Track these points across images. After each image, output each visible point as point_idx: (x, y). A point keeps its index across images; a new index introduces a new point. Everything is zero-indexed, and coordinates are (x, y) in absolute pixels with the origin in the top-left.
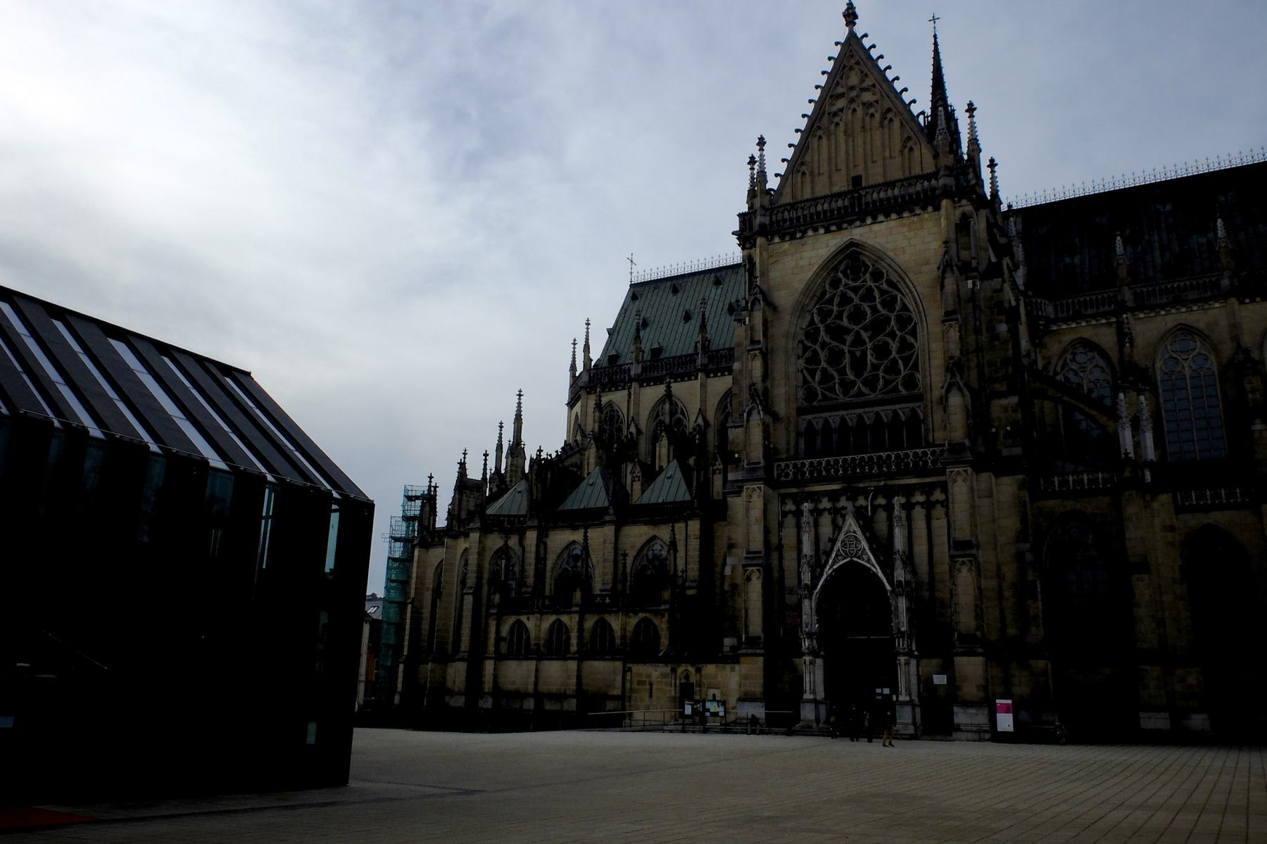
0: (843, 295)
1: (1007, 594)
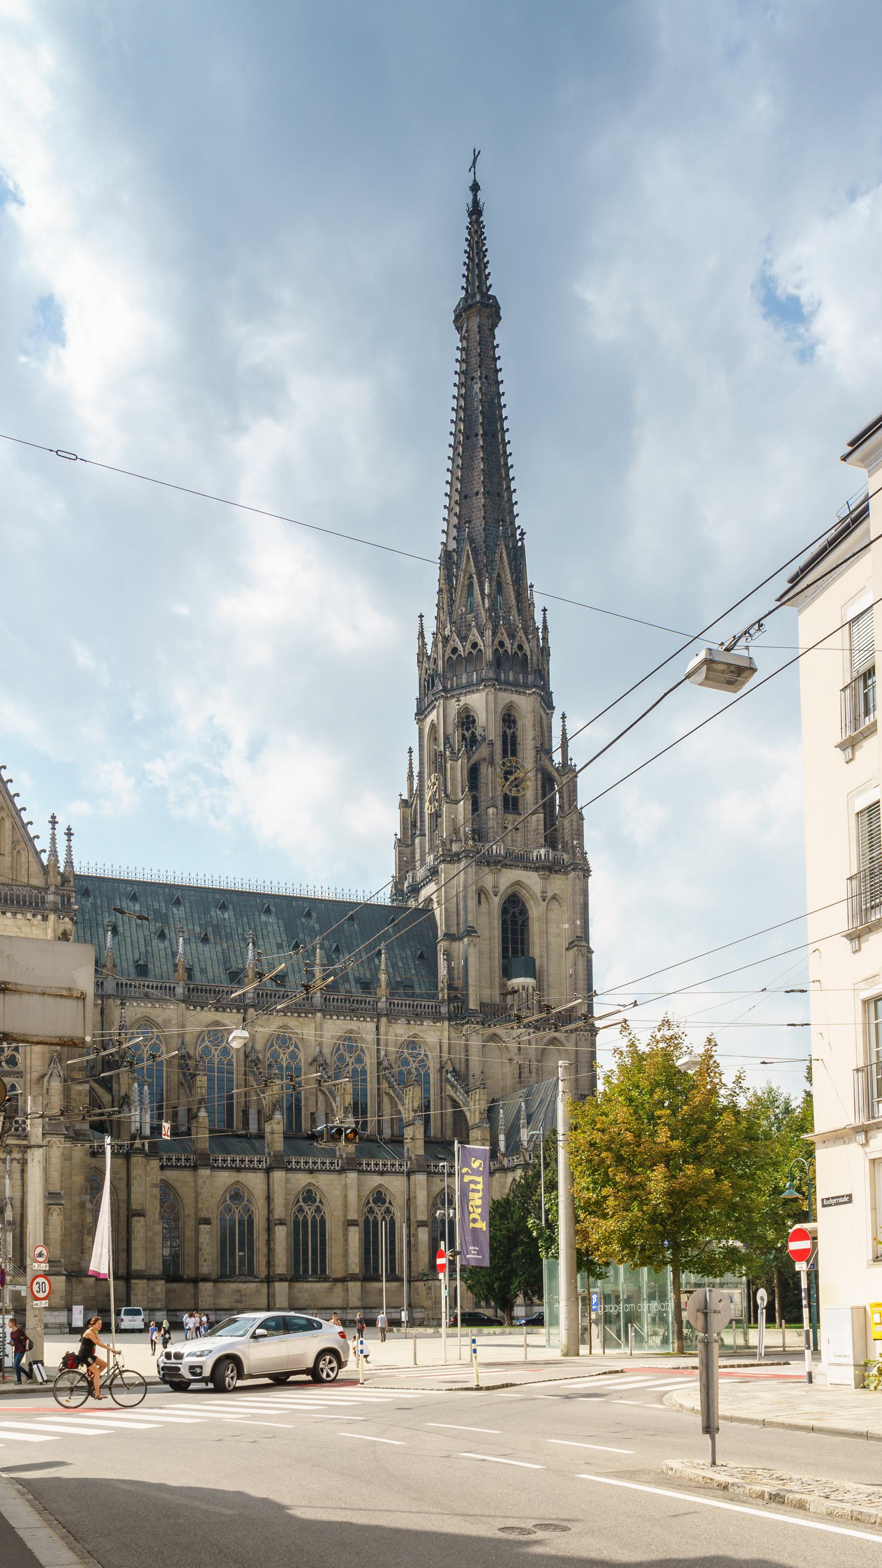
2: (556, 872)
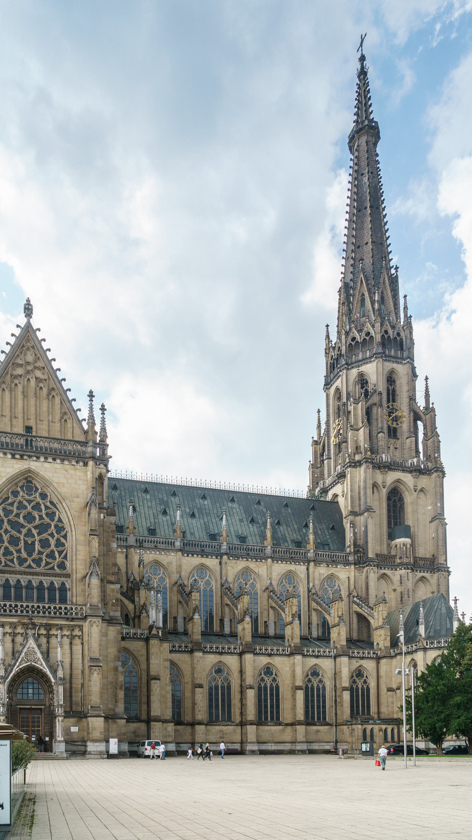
0: (20, 502)
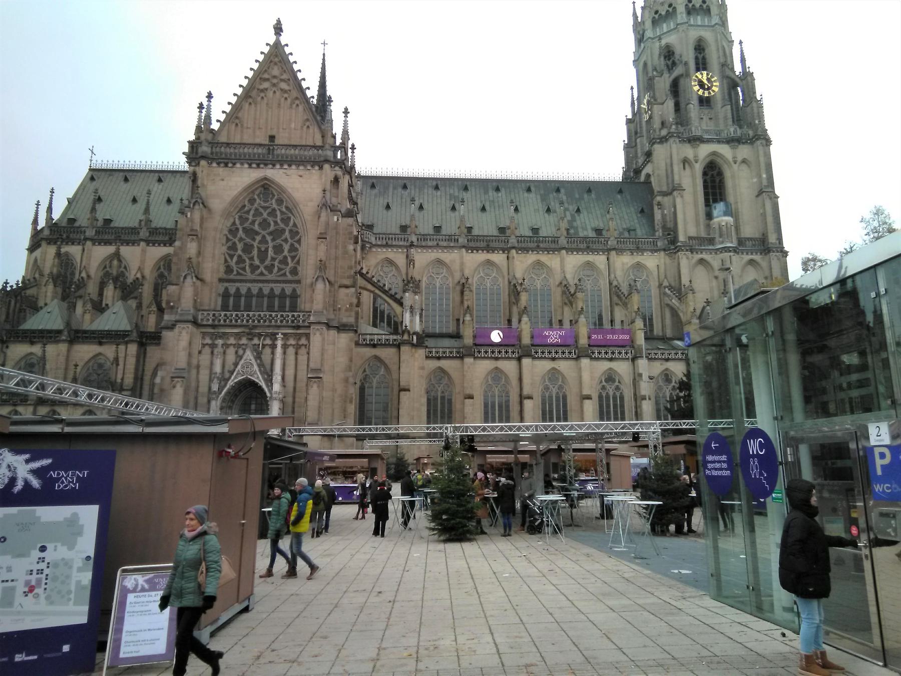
0: (257, 210)
1: (337, 400)
2: (743, 143)
